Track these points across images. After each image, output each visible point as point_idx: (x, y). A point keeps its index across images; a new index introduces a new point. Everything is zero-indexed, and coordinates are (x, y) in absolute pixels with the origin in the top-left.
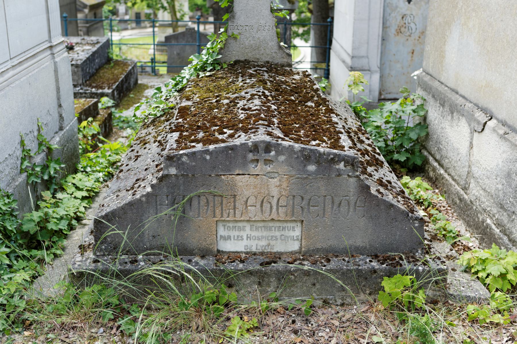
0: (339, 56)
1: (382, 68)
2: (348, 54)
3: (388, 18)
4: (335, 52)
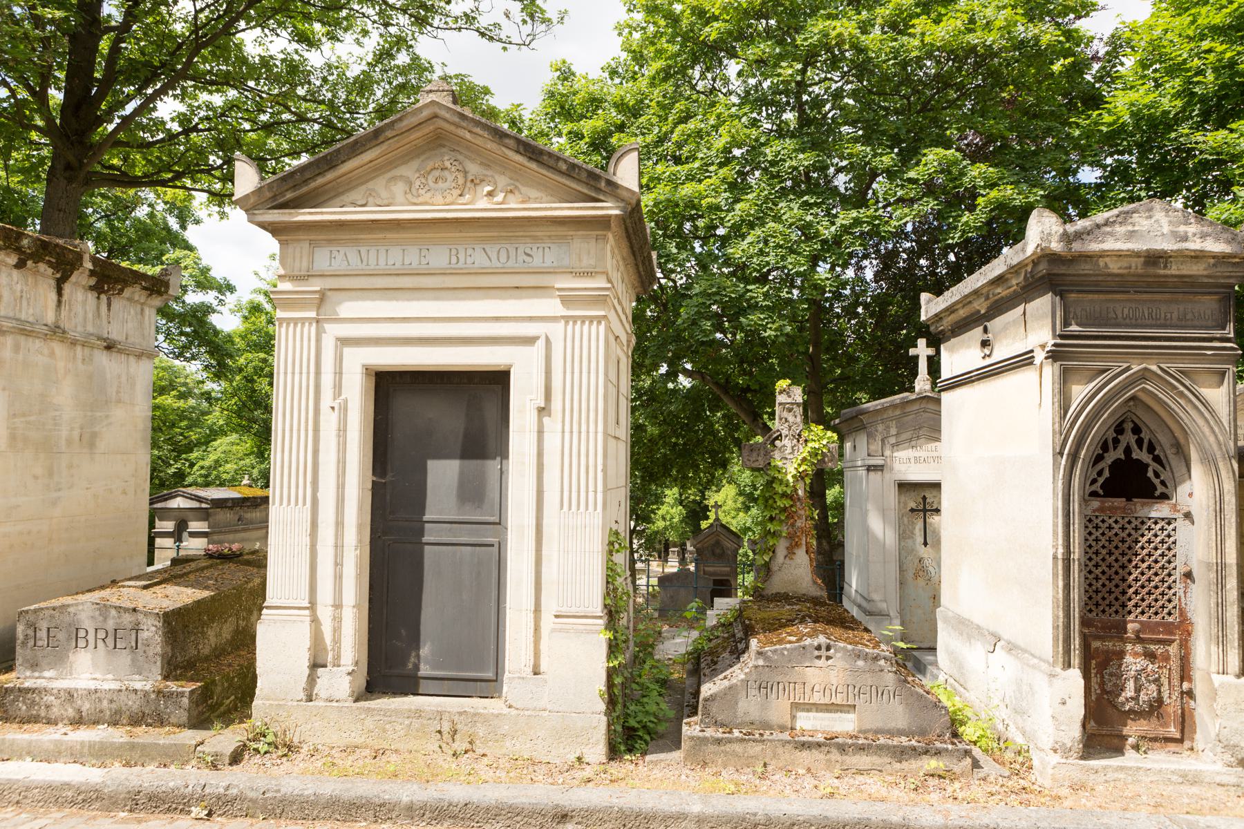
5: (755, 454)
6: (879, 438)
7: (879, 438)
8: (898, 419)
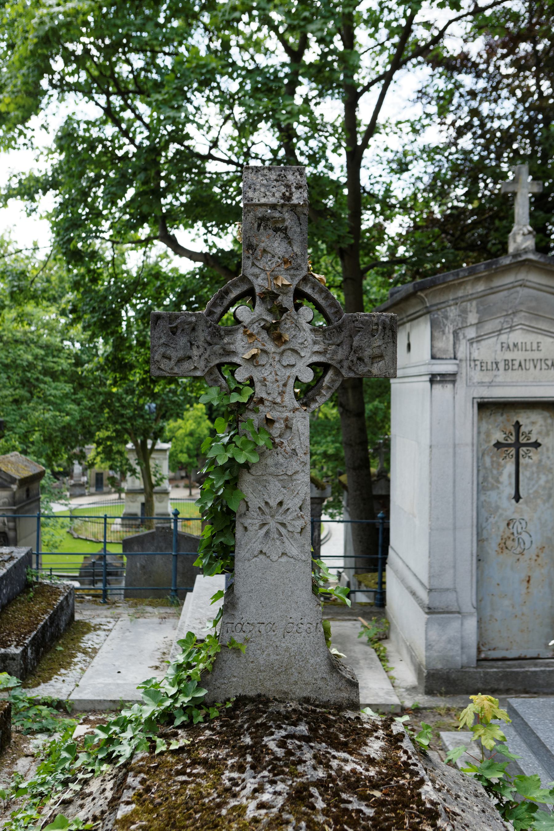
0: (403, 581)
1: (479, 608)
2: (422, 584)
3: (484, 525)
4: (396, 572)
5: (183, 341)
6: (450, 328)
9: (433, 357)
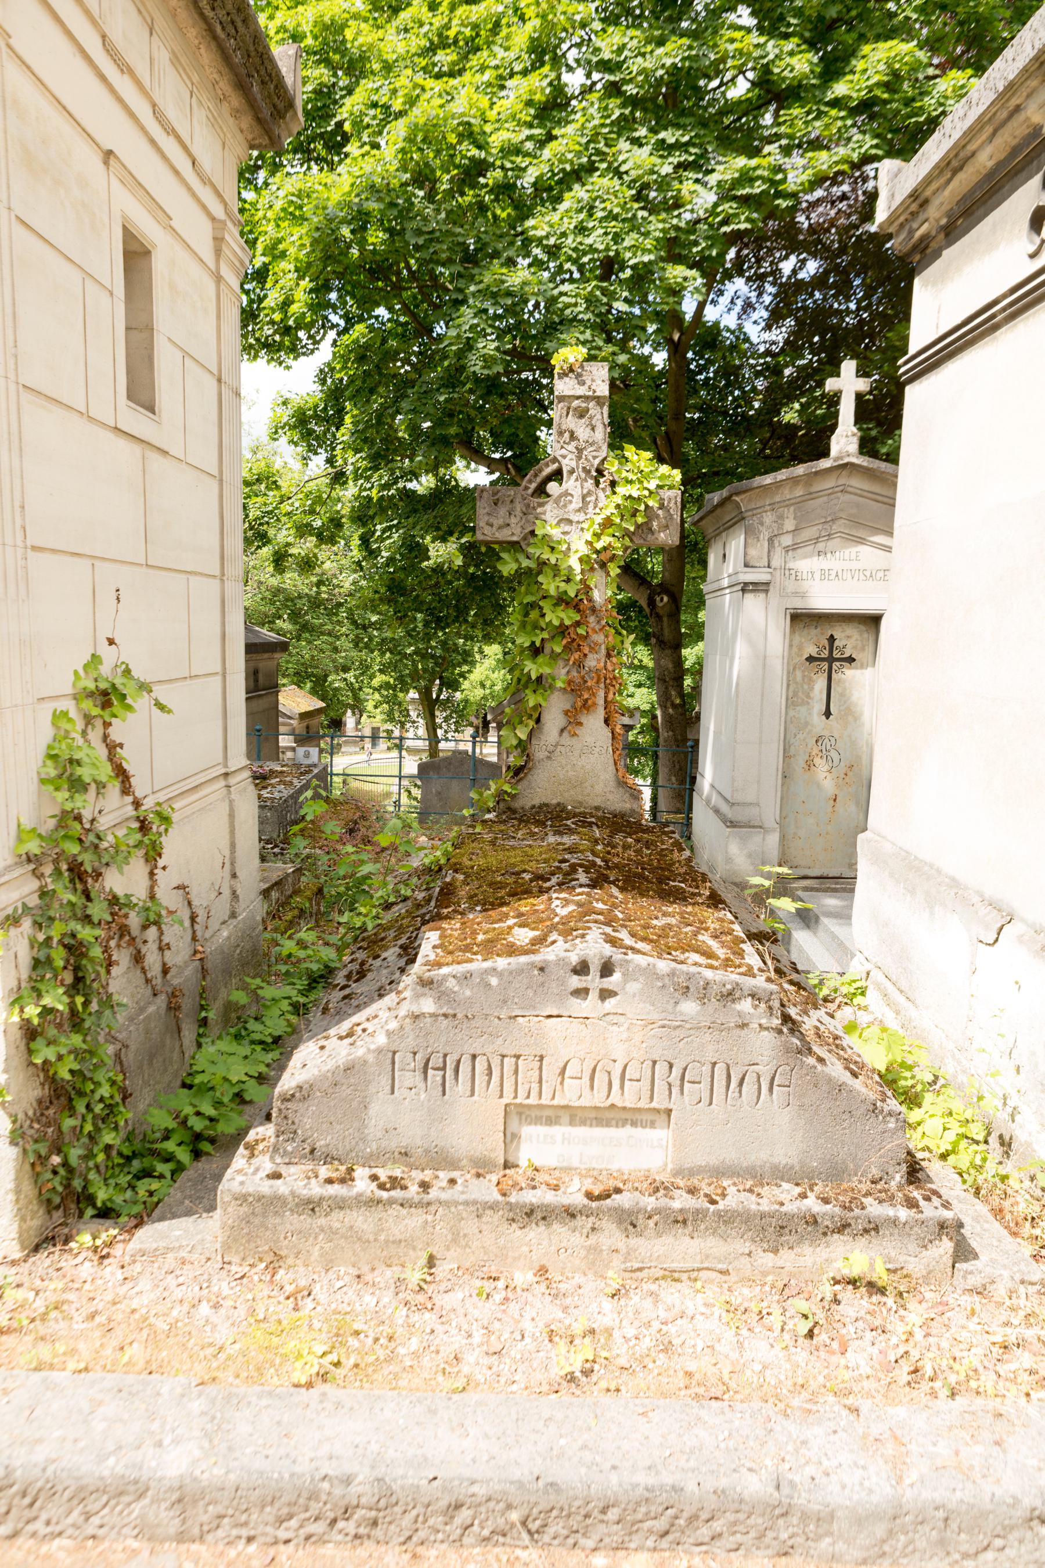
6: (765, 535)
7: (765, 535)
8: (799, 503)
9: (746, 565)
